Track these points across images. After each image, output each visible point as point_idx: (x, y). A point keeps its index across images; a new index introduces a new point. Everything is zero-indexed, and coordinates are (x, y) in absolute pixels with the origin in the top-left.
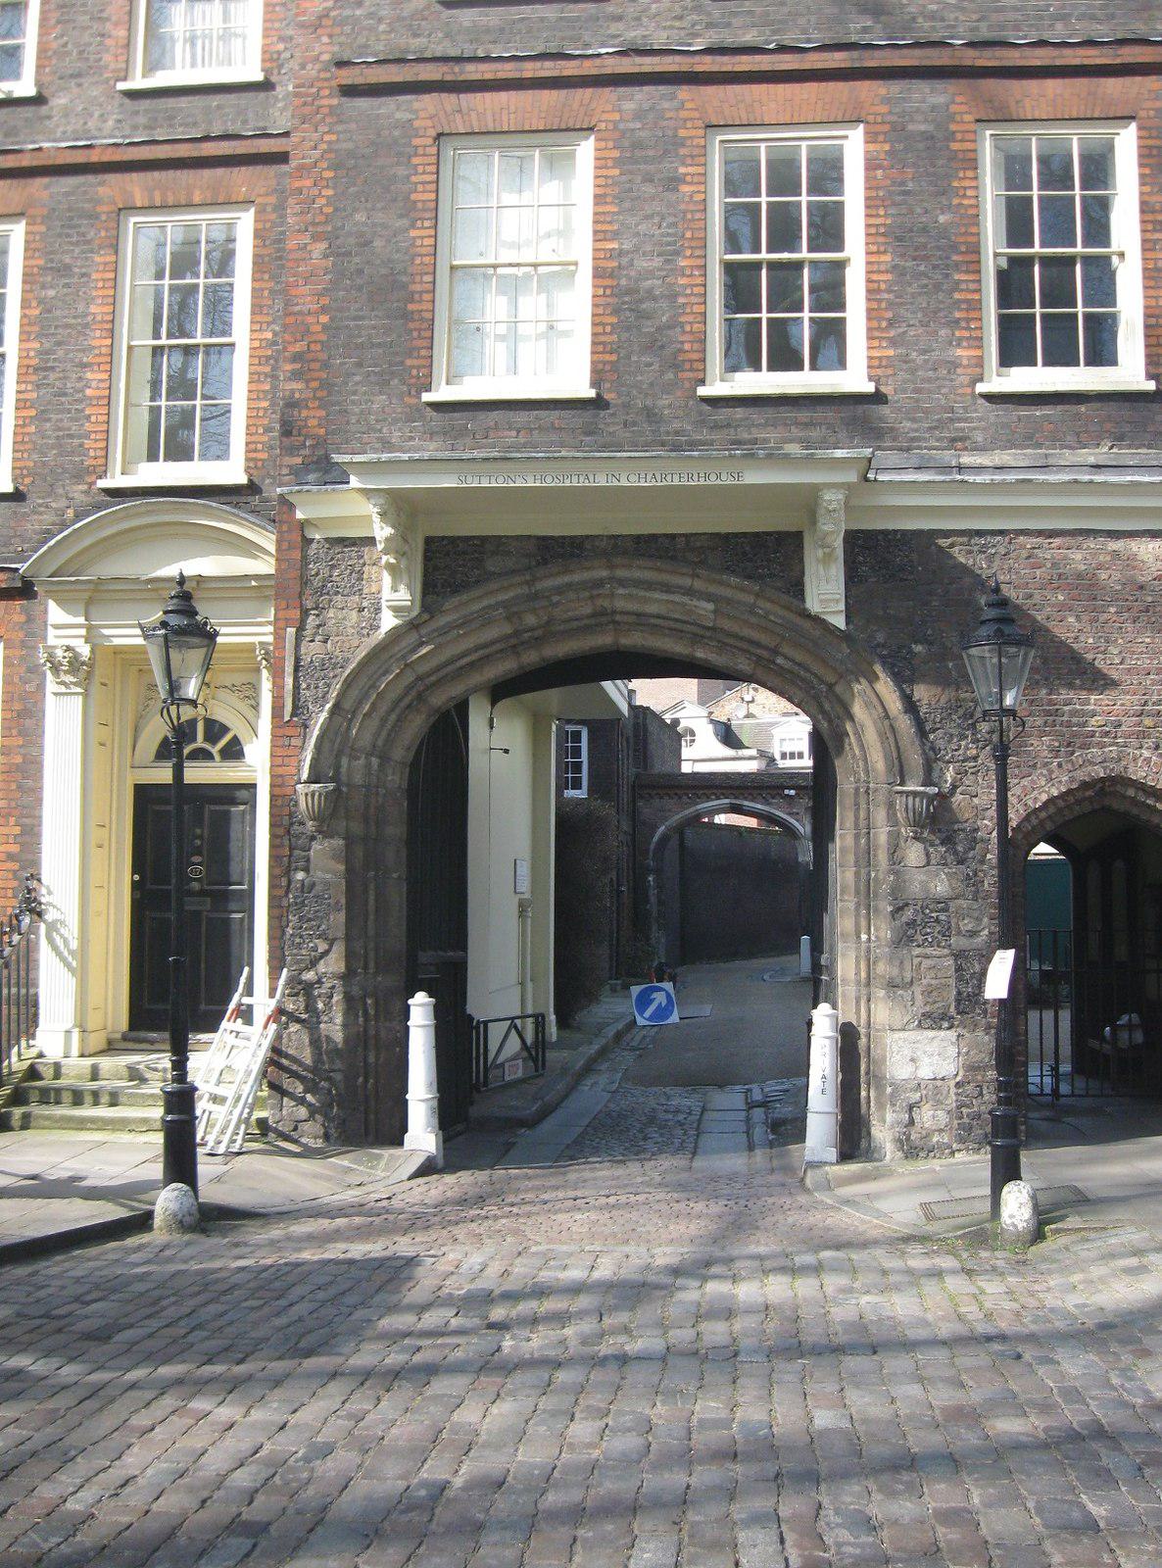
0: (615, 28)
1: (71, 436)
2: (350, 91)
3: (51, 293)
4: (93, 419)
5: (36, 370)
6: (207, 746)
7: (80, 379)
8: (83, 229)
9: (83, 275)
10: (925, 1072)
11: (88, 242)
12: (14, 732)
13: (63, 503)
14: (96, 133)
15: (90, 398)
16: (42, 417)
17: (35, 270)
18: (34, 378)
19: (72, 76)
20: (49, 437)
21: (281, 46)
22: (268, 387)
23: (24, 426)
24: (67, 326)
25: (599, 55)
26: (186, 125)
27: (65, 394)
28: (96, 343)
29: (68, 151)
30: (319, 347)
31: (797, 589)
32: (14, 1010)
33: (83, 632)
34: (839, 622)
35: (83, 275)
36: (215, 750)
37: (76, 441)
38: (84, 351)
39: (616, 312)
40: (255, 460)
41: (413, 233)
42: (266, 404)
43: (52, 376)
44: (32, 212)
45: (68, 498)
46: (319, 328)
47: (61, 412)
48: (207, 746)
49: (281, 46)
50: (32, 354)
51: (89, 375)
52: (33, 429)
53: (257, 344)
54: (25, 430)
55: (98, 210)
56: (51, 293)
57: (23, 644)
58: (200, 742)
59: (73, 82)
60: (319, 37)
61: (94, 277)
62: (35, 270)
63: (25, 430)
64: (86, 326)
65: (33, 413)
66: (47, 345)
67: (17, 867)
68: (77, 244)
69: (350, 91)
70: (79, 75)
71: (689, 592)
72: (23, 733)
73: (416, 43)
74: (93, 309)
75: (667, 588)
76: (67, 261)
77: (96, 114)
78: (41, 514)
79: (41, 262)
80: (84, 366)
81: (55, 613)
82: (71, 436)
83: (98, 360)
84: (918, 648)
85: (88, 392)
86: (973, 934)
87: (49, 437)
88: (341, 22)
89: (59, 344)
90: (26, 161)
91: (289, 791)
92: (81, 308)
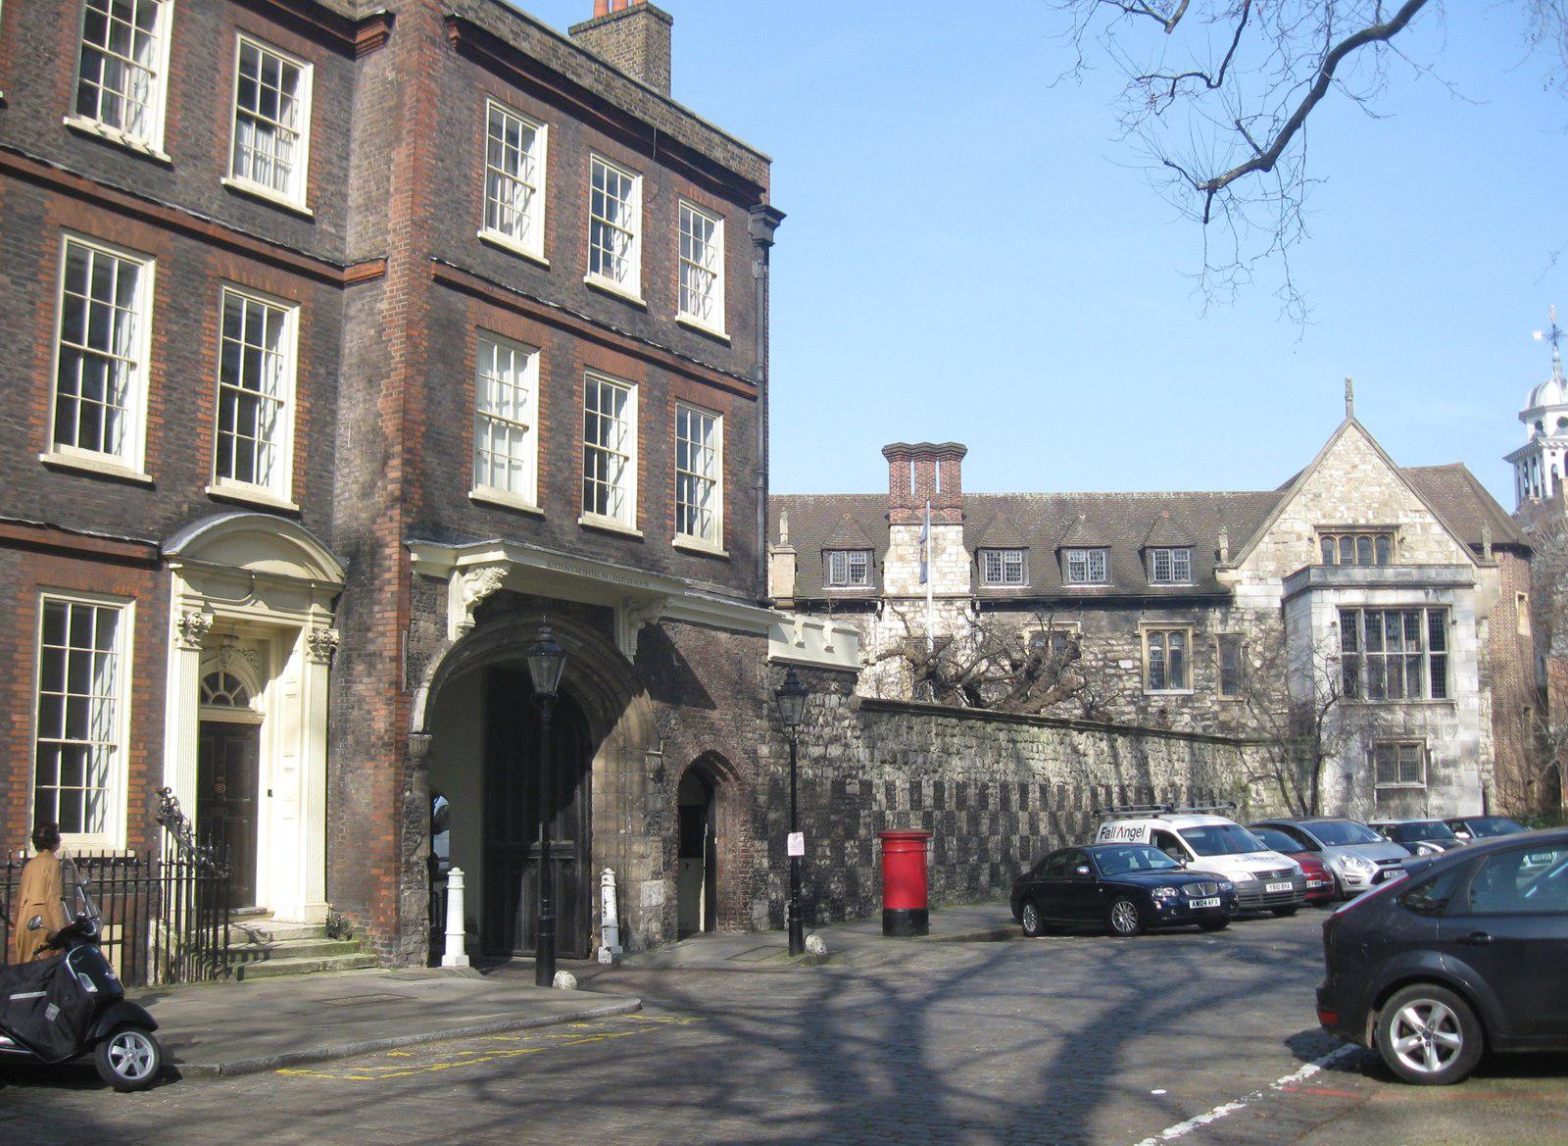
0: (552, 290)
1: (187, 447)
2: (439, 280)
3: (175, 328)
4: (202, 437)
5: (165, 387)
6: (226, 693)
7: (194, 403)
8: (196, 284)
9: (196, 321)
10: (654, 903)
11: (199, 295)
12: (144, 675)
13: (180, 498)
14: (207, 211)
15: (201, 420)
16: (167, 426)
17: (164, 306)
18: (162, 393)
19: (191, 156)
20: (172, 443)
21: (319, 194)
22: (306, 443)
23: (155, 430)
24: (186, 358)
25: (548, 306)
26: (263, 229)
27: (183, 412)
28: (204, 378)
29: (193, 220)
30: (419, 447)
31: (610, 637)
32: (131, 895)
33: (202, 603)
34: (632, 660)
35: (196, 321)
36: (231, 698)
37: (189, 451)
38: (195, 381)
39: (549, 464)
40: (298, 493)
41: (465, 386)
42: (305, 455)
43: (175, 395)
44: (162, 256)
45: (184, 496)
46: (419, 434)
47: (182, 426)
48: (226, 693)
49: (319, 194)
50: (161, 373)
51: (200, 402)
52: (161, 434)
53: (301, 409)
54: (156, 433)
55: (208, 272)
56: (175, 328)
57: (151, 606)
58: (222, 691)
59: (192, 160)
60: (422, 234)
61: (204, 324)
62: (164, 306)
63: (156, 433)
64: (198, 362)
65: (161, 421)
66: (172, 370)
67: (144, 782)
68: (192, 294)
69: (439, 280)
70: (195, 158)
71: (575, 636)
72: (150, 676)
73: (468, 261)
74: (204, 351)
75: (568, 633)
76: (185, 306)
77: (207, 195)
78: (166, 503)
79: (168, 300)
80: (196, 393)
81: (178, 585)
82: (187, 447)
83: (205, 391)
84: (653, 678)
85: (200, 415)
86: (668, 829)
87: (172, 443)
88: (433, 229)
89: (179, 370)
90: (164, 215)
91: (404, 738)
92: (195, 347)
